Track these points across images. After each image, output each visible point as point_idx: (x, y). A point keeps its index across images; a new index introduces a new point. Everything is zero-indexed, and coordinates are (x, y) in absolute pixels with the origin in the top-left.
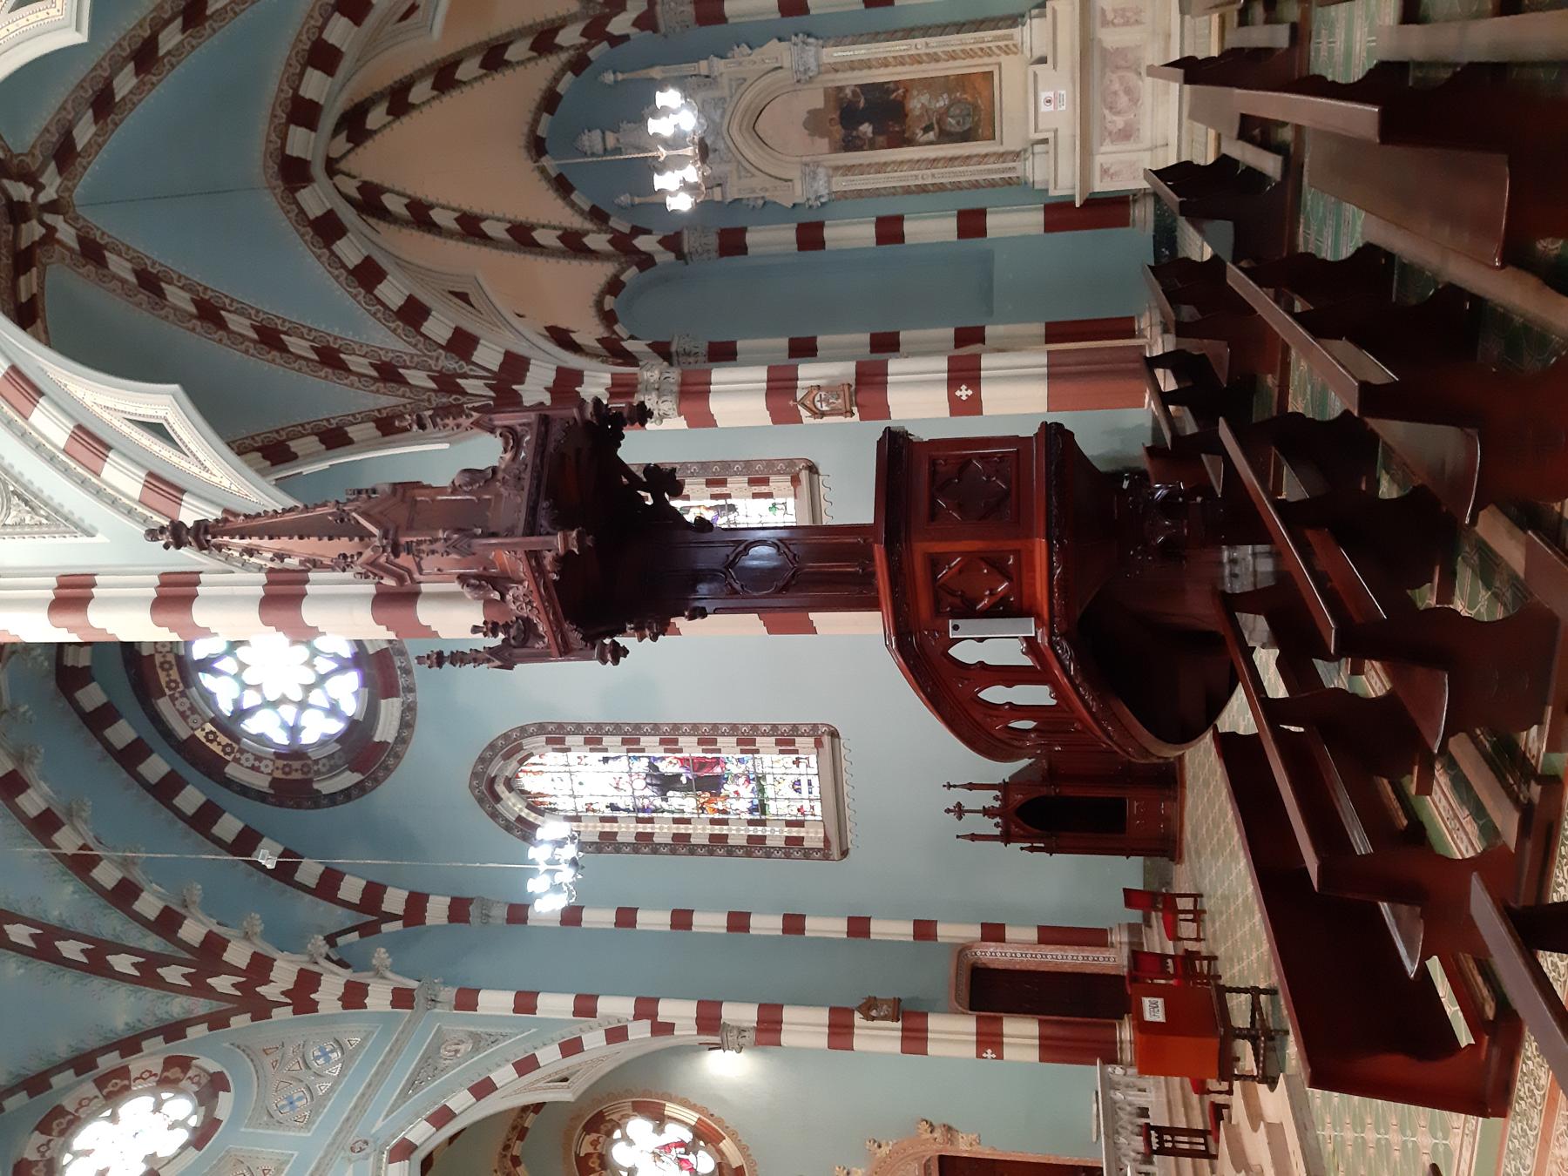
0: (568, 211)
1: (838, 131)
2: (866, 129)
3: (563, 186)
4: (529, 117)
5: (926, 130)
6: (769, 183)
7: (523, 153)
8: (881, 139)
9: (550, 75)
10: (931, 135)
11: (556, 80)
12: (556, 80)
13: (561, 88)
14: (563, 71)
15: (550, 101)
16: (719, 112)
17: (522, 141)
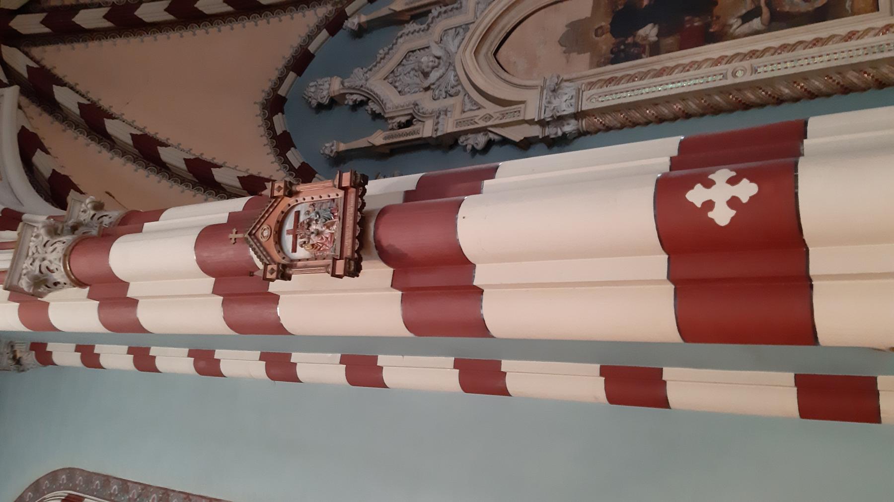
0: (276, 166)
1: (606, 42)
2: (649, 32)
3: (282, 144)
4: (275, 75)
5: (746, 18)
6: (491, 108)
7: (258, 110)
8: (670, 40)
9: (304, 32)
10: (756, 23)
11: (311, 37)
12: (311, 37)
13: (312, 48)
14: (319, 29)
15: (301, 62)
16: (457, 41)
17: (261, 97)
